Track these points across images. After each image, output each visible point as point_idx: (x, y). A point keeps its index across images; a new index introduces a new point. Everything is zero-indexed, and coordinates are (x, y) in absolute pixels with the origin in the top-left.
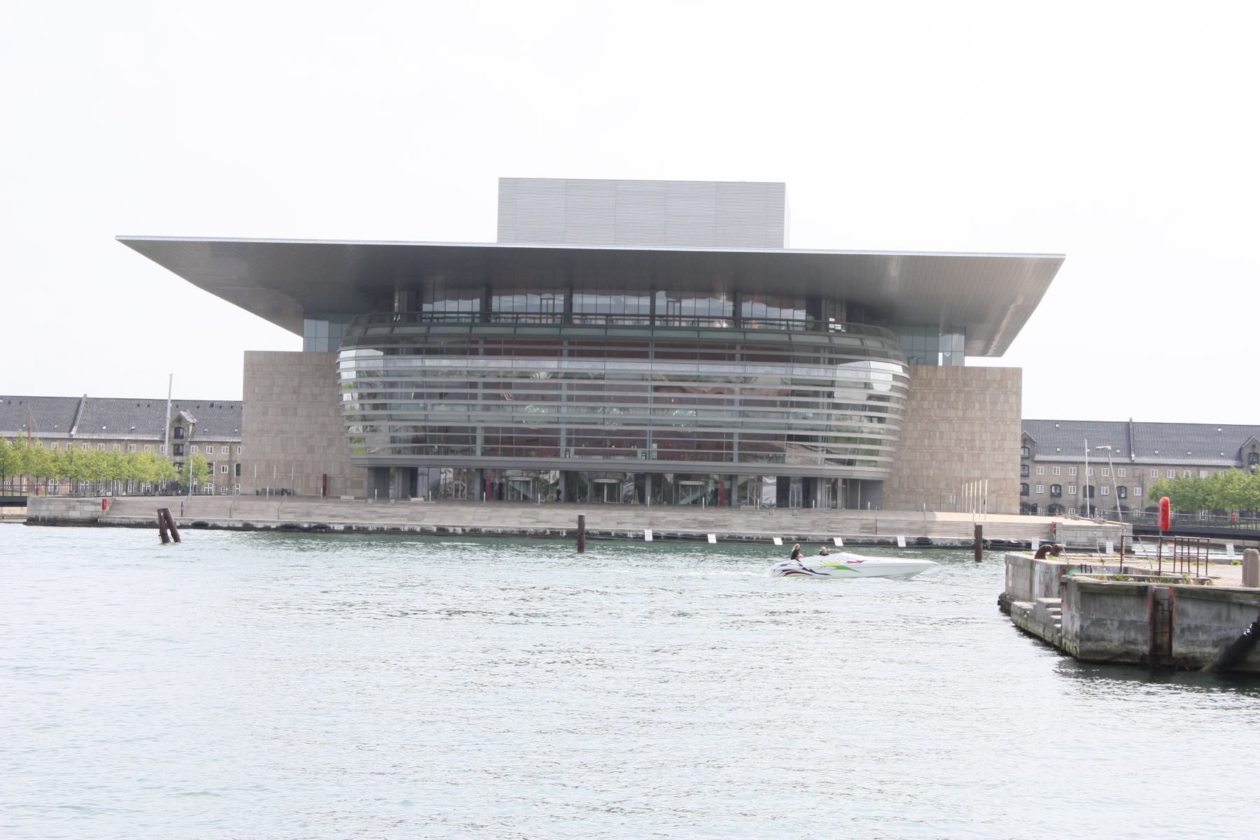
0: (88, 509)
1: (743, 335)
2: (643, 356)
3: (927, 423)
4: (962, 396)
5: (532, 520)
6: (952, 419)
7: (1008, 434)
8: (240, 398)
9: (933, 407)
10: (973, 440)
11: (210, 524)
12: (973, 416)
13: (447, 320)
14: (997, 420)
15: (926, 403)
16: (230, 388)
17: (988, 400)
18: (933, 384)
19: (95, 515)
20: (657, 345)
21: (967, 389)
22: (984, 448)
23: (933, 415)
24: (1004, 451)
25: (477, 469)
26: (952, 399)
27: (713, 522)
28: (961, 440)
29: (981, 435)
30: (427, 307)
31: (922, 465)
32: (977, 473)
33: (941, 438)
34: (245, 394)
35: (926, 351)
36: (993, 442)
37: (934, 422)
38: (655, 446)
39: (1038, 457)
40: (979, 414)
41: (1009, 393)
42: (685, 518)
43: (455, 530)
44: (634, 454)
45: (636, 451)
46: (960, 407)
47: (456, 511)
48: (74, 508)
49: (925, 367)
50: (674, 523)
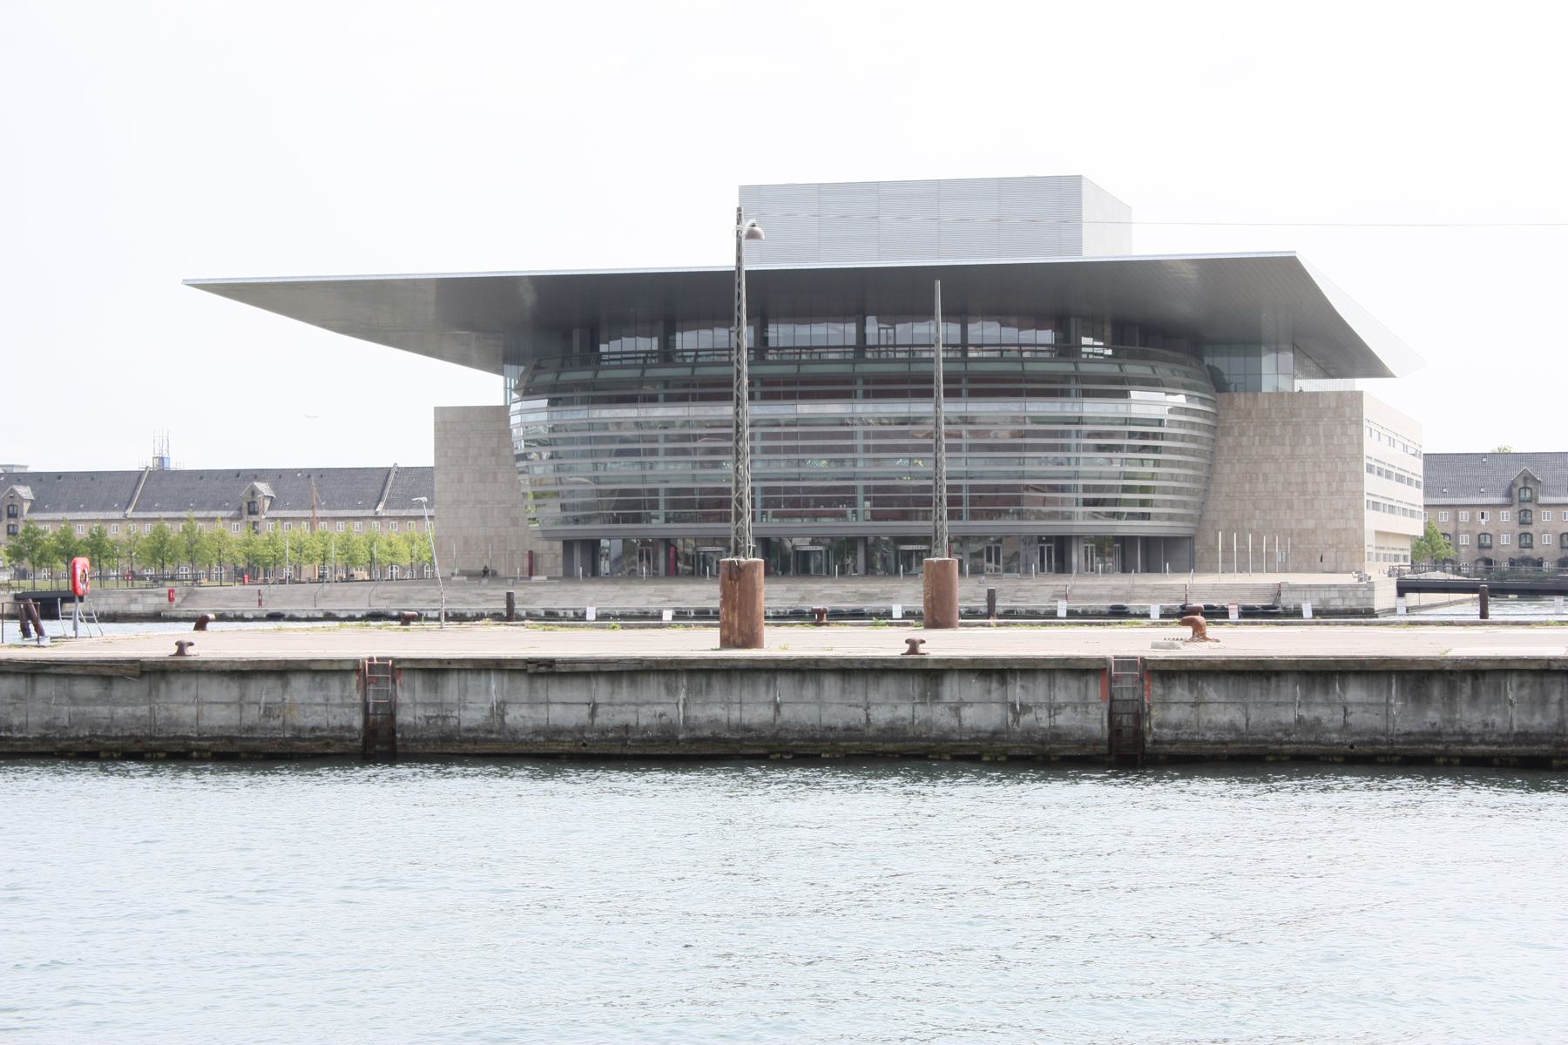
0: (150, 603)
1: (964, 365)
2: (847, 395)
3: (1247, 464)
4: (1289, 428)
5: (664, 599)
6: (1276, 457)
8: (431, 464)
9: (1254, 444)
10: (1305, 483)
11: (287, 615)
12: (1304, 453)
13: (624, 362)
14: (1334, 456)
15: (1245, 440)
16: (419, 451)
17: (1321, 433)
18: (1254, 415)
19: (159, 608)
20: (866, 382)
21: (1294, 420)
22: (1319, 492)
23: (1254, 453)
24: (1343, 494)
25: (661, 540)
26: (1278, 434)
27: (876, 594)
28: (1290, 483)
29: (1314, 477)
30: (603, 348)
31: (1243, 516)
32: (1310, 524)
33: (1265, 481)
34: (437, 458)
35: (1245, 375)
36: (1329, 484)
37: (1256, 462)
38: (868, 504)
39: (1542, 499)
40: (1311, 450)
41: (1347, 423)
42: (845, 590)
43: (565, 613)
44: (843, 515)
45: (845, 511)
46: (1287, 443)
47: (578, 590)
48: (135, 601)
49: (1242, 395)
50: (830, 596)
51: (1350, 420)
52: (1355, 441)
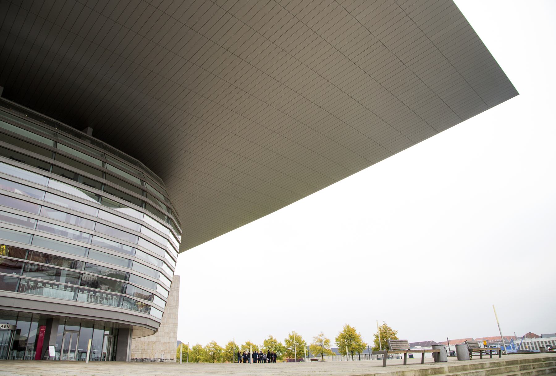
7: (172, 315)
41: (173, 290)
51: (174, 289)
52: (176, 299)
